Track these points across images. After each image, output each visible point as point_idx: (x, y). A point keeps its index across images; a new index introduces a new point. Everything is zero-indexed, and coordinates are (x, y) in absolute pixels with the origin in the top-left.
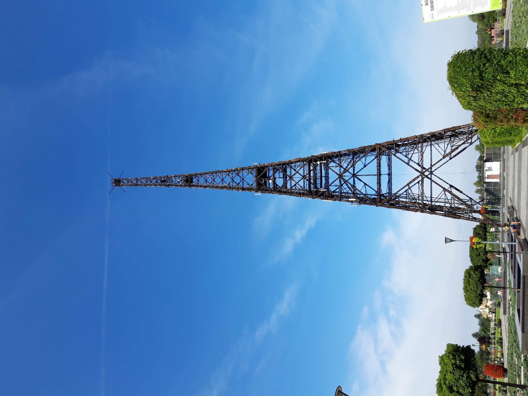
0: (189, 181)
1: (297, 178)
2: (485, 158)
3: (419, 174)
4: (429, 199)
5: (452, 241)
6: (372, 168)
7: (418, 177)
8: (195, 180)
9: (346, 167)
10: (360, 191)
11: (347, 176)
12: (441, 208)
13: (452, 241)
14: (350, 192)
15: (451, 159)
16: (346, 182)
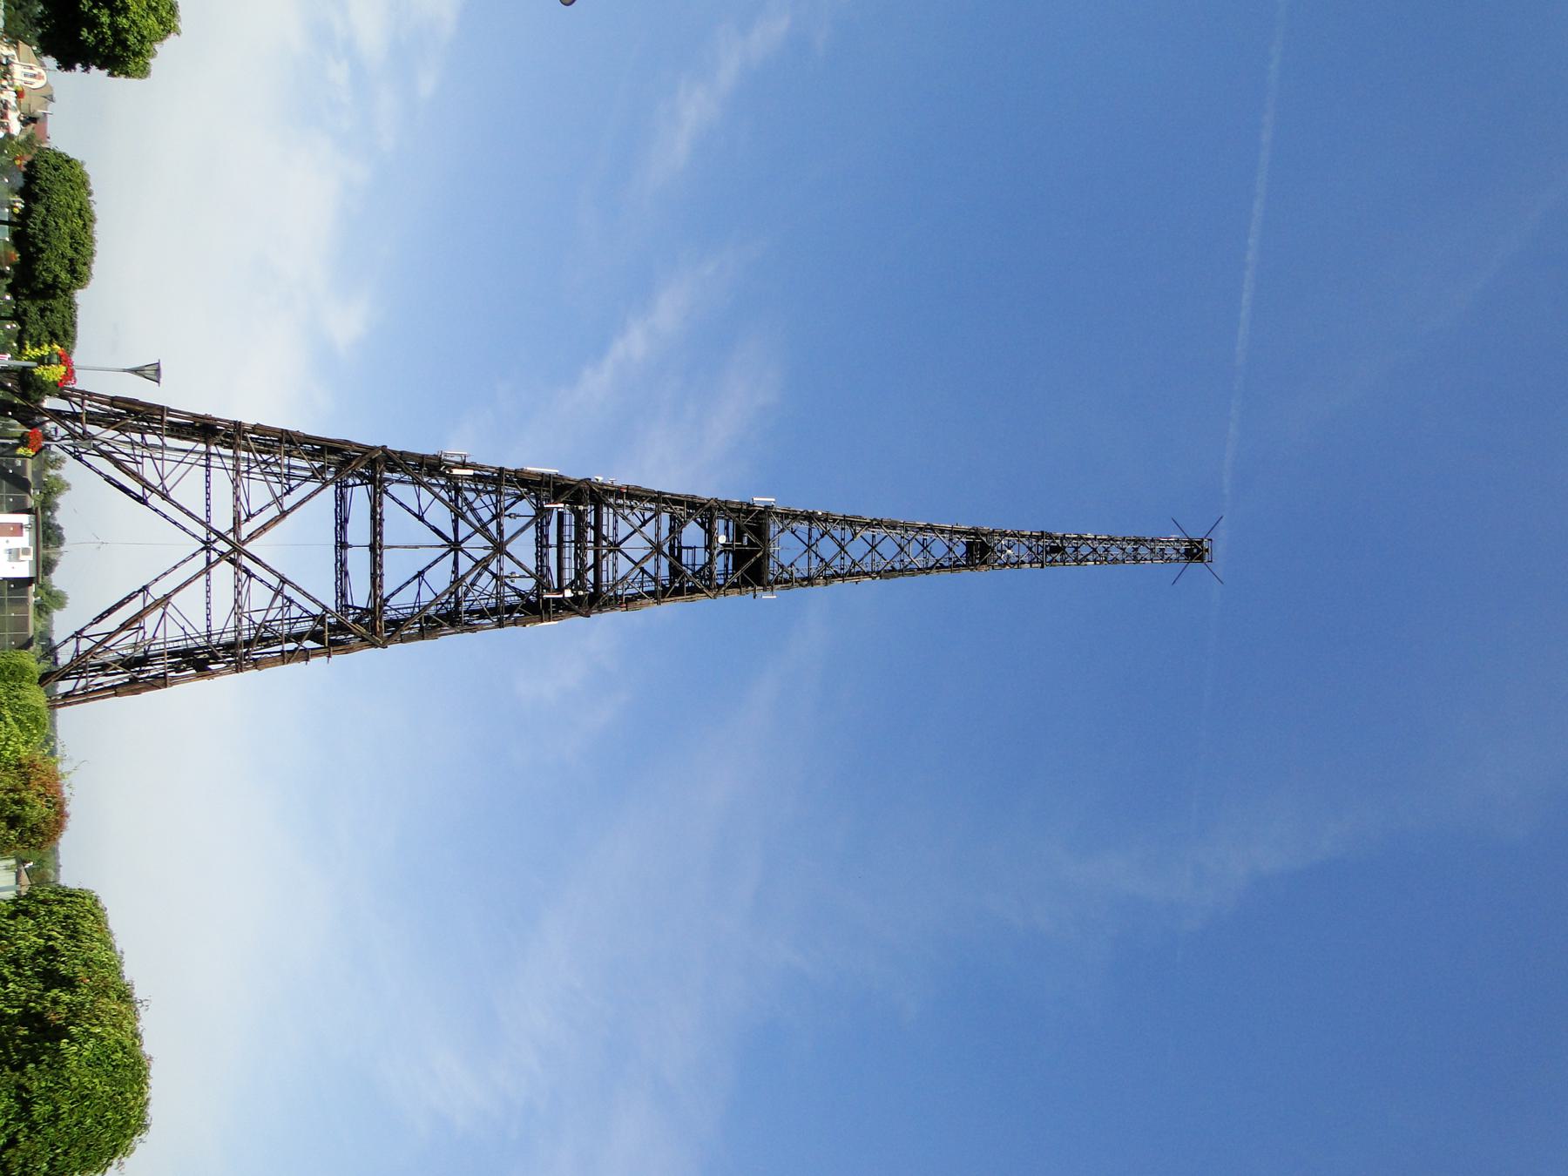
0: (980, 550)
1: (637, 547)
2: (33, 588)
4: (215, 461)
5: (135, 371)
6: (396, 569)
7: (251, 537)
8: (960, 550)
9: (480, 575)
10: (436, 496)
11: (477, 546)
12: (178, 431)
13: (135, 371)
14: (471, 496)
15: (145, 588)
16: (482, 529)
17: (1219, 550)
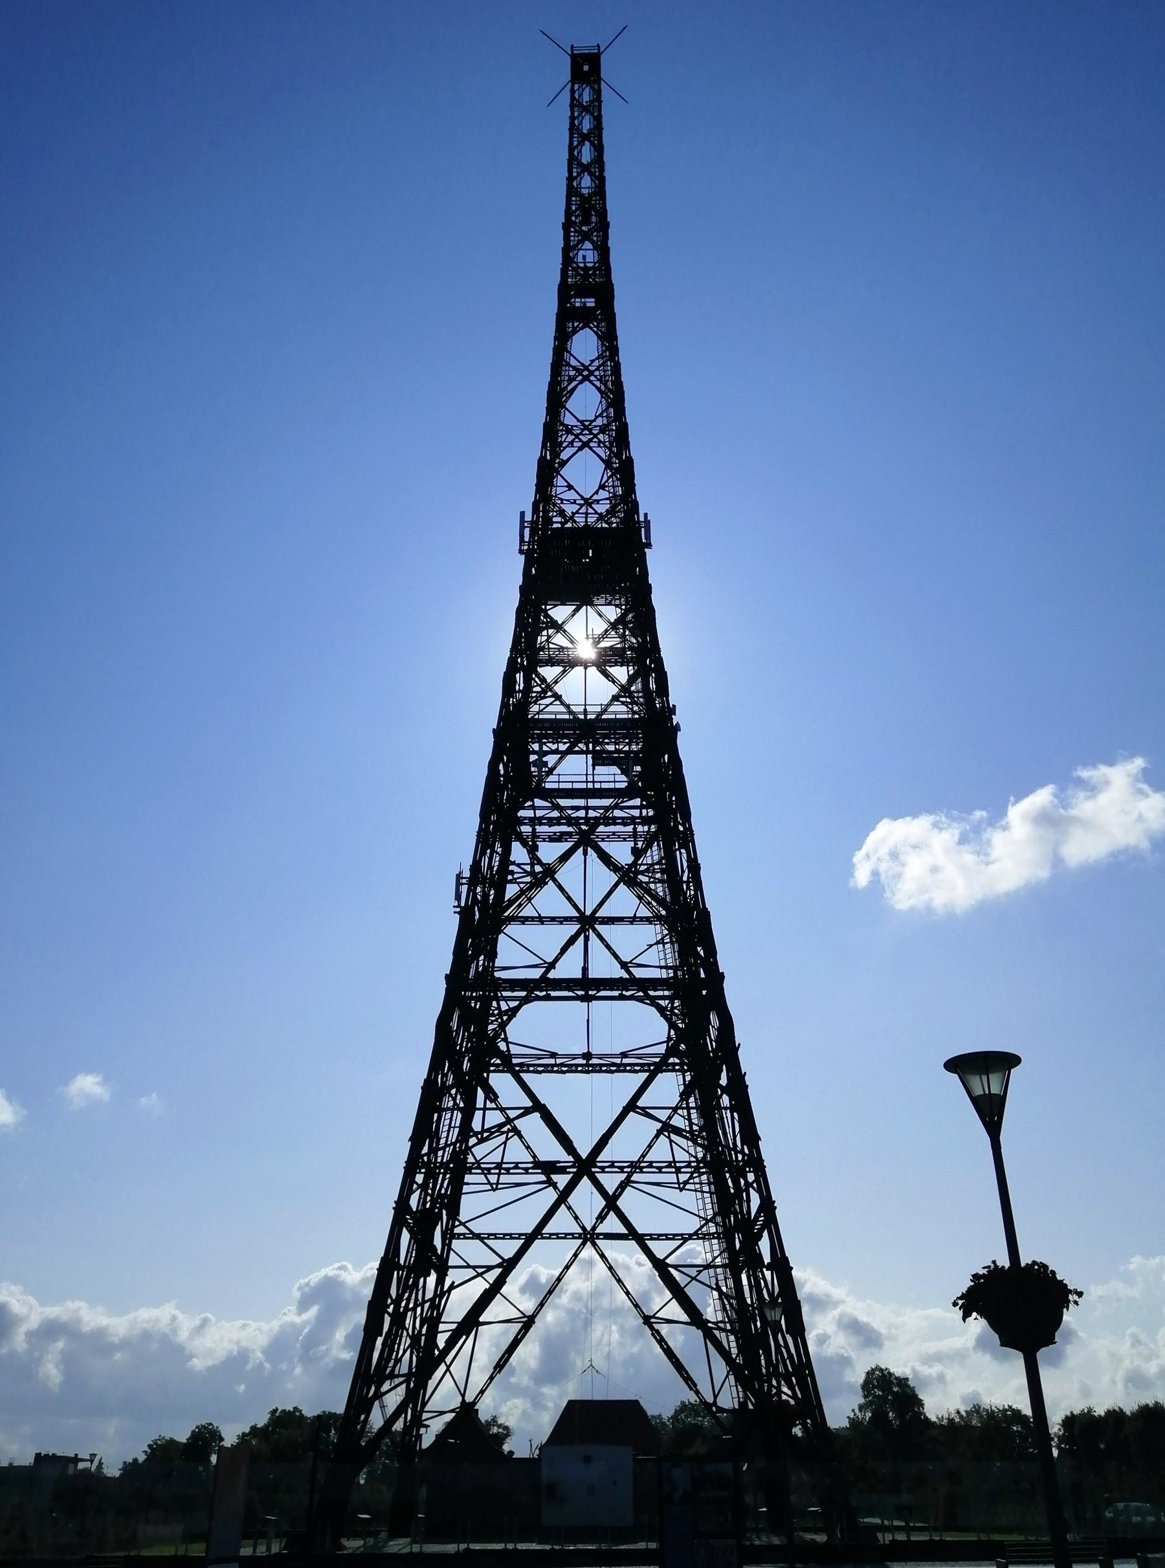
7: (567, 1143)
12: (432, 1261)
17: (585, 42)
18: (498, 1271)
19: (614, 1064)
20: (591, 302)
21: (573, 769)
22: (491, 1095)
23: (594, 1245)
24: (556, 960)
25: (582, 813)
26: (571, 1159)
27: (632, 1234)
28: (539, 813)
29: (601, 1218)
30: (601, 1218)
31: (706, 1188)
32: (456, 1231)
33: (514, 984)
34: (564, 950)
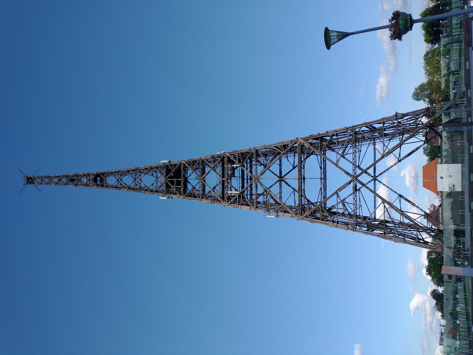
3: (350, 179)
17: (23, 180)
18: (386, 204)
19: (324, 172)
20: (99, 179)
21: (236, 182)
22: (333, 207)
23: (377, 176)
24: (292, 188)
25: (249, 181)
26: (352, 183)
27: (374, 165)
28: (249, 193)
29: (369, 175)
30: (369, 175)
31: (360, 144)
32: (373, 217)
33: (300, 200)
34: (289, 186)
